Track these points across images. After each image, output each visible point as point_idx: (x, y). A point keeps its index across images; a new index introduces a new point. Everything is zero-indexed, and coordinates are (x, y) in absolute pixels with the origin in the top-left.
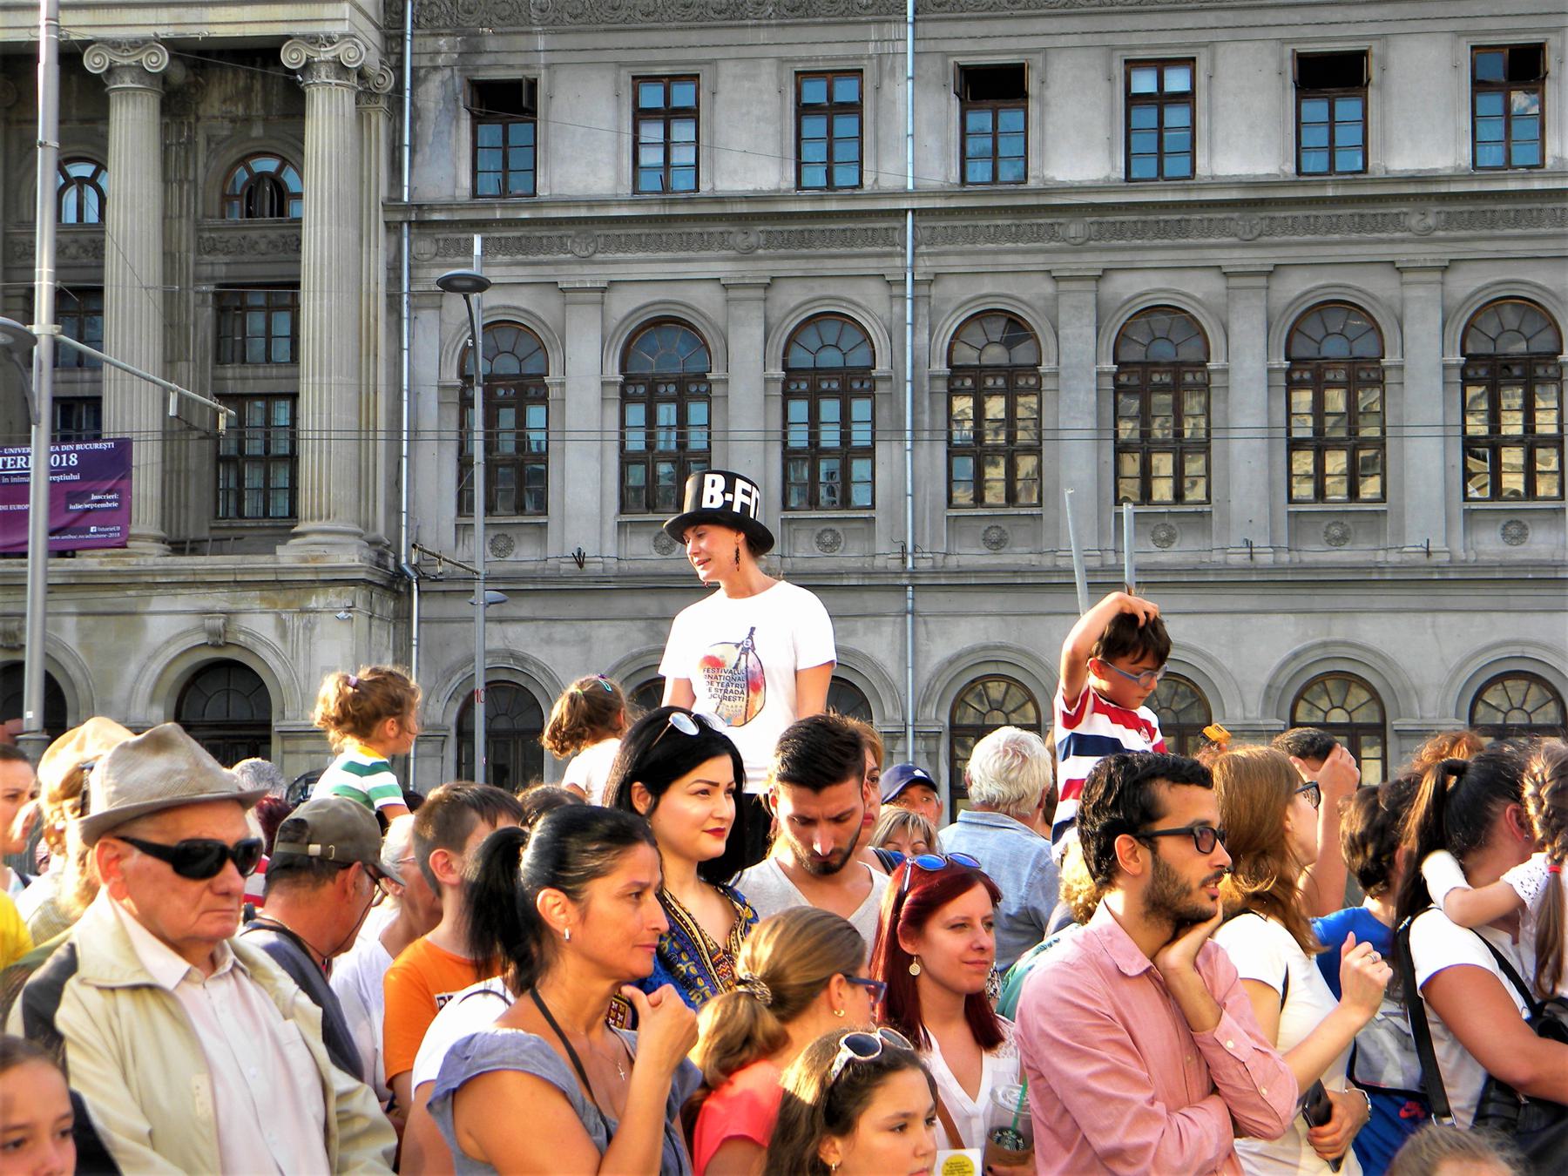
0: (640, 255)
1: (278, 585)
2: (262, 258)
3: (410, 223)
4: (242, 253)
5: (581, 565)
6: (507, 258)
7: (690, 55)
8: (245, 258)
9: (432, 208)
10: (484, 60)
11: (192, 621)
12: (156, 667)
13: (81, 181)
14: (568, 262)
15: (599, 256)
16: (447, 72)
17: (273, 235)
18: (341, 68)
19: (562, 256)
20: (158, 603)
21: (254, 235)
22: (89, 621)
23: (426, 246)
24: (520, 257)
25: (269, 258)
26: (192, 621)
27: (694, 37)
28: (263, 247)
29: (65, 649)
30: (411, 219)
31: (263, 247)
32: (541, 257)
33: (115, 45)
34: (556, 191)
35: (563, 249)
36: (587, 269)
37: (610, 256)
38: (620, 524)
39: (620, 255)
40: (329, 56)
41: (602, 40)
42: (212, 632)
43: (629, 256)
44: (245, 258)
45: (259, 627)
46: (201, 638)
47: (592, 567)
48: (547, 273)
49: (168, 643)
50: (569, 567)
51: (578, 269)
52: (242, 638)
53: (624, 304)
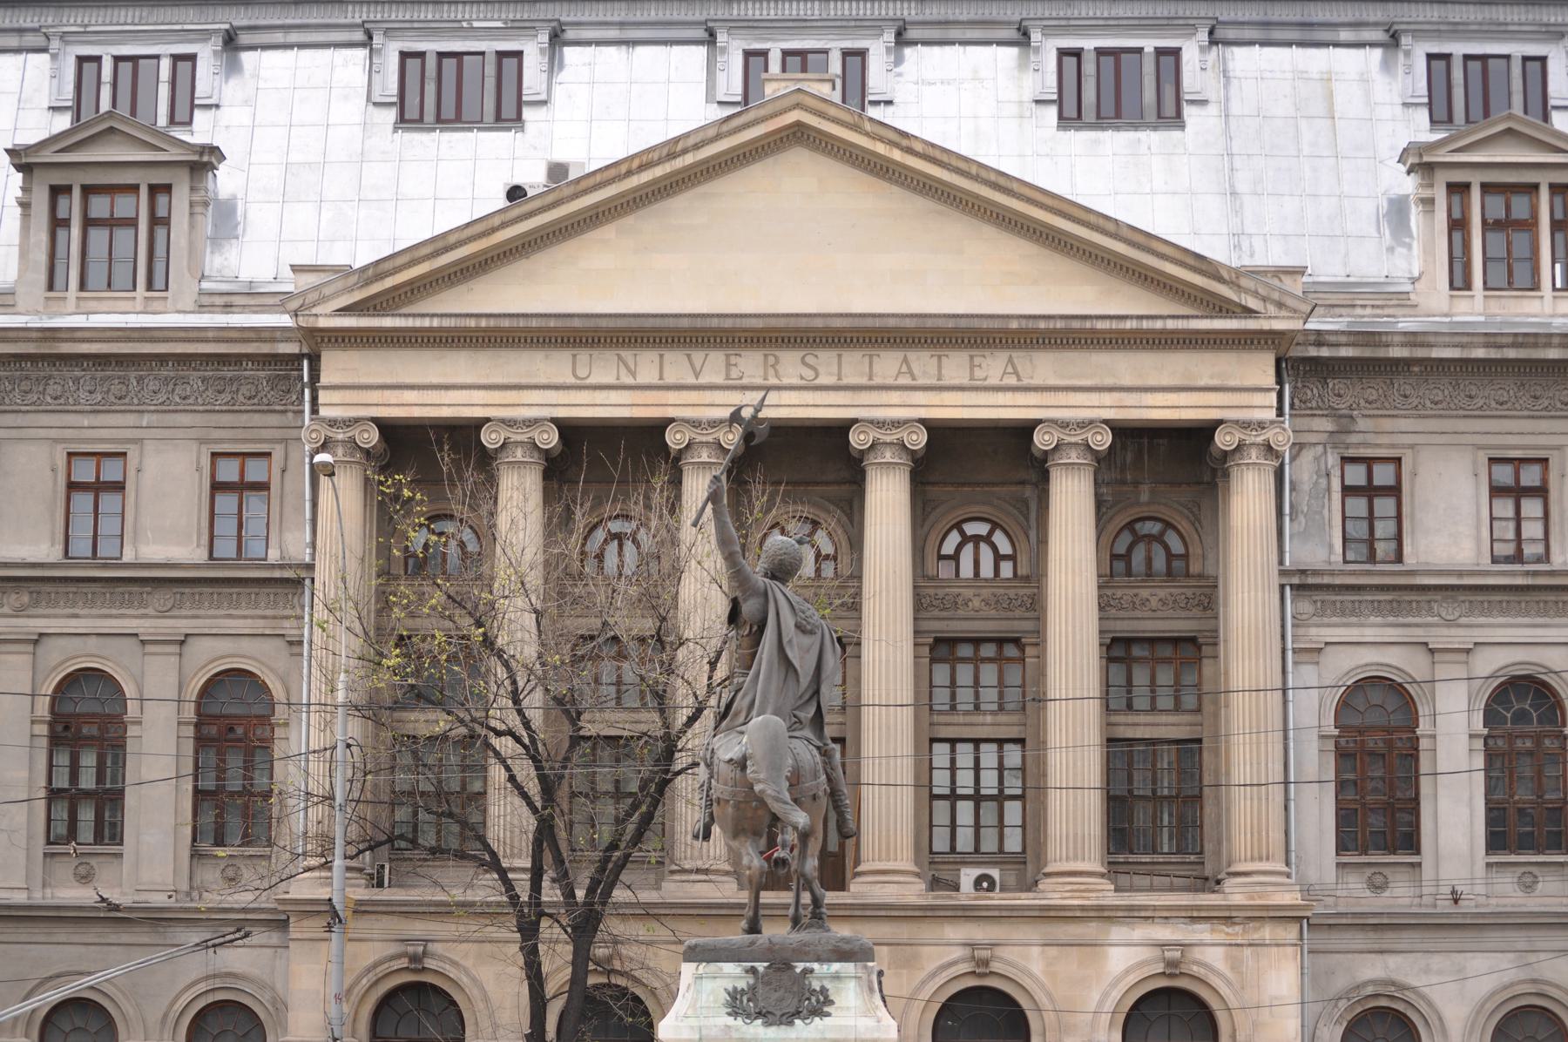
0: (1501, 620)
1: (1226, 917)
2: (1150, 614)
3: (1291, 586)
4: (1134, 608)
5: (1456, 901)
6: (1379, 619)
7: (1542, 440)
8: (1138, 614)
9: (1316, 573)
10: (1354, 439)
11: (1145, 953)
12: (1116, 994)
13: (977, 539)
14: (1437, 625)
15: (1463, 620)
16: (1320, 449)
17: (1162, 593)
18: (1268, 448)
19: (1430, 619)
20: (1118, 933)
21: (1144, 593)
22: (1053, 951)
23: (1306, 607)
24: (1391, 619)
25: (1159, 614)
26: (1145, 953)
27: (1544, 425)
28: (1154, 603)
29: (1031, 975)
30: (1301, 585)
31: (1154, 603)
32: (1410, 620)
33: (1064, 425)
34: (1422, 559)
35: (1430, 612)
36: (1453, 631)
37: (1473, 620)
38: (1488, 865)
39: (1482, 620)
40: (1260, 440)
41: (1462, 425)
42: (1171, 964)
43: (1491, 620)
44: (1138, 614)
45: (1212, 957)
46: (1160, 968)
47: (1466, 906)
48: (1418, 634)
49: (1127, 972)
50: (1445, 906)
51: (1445, 631)
52: (1195, 968)
53: (1490, 663)
